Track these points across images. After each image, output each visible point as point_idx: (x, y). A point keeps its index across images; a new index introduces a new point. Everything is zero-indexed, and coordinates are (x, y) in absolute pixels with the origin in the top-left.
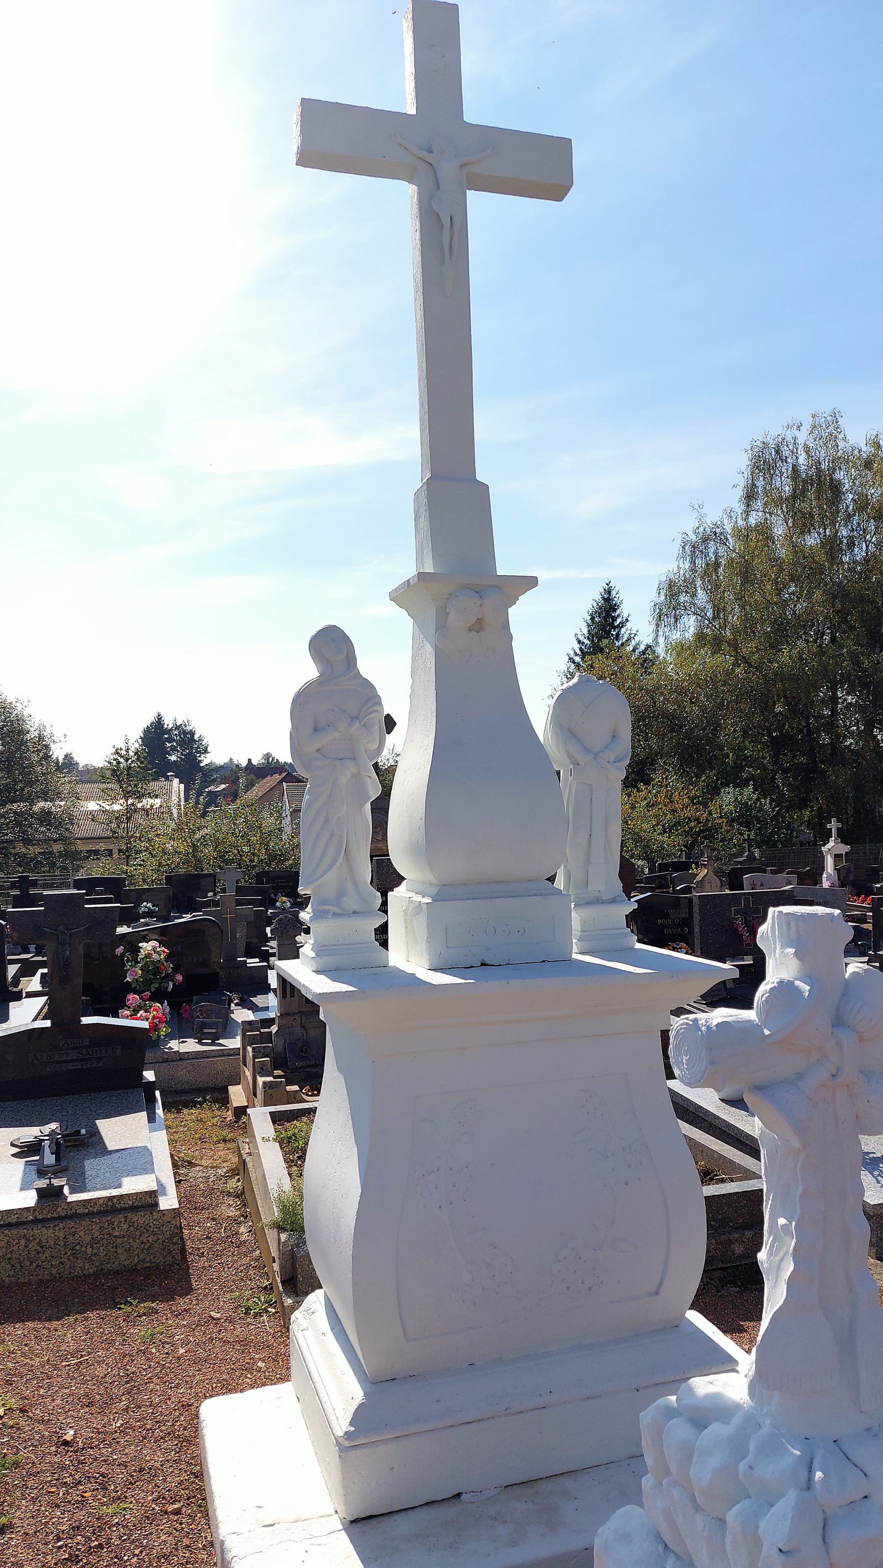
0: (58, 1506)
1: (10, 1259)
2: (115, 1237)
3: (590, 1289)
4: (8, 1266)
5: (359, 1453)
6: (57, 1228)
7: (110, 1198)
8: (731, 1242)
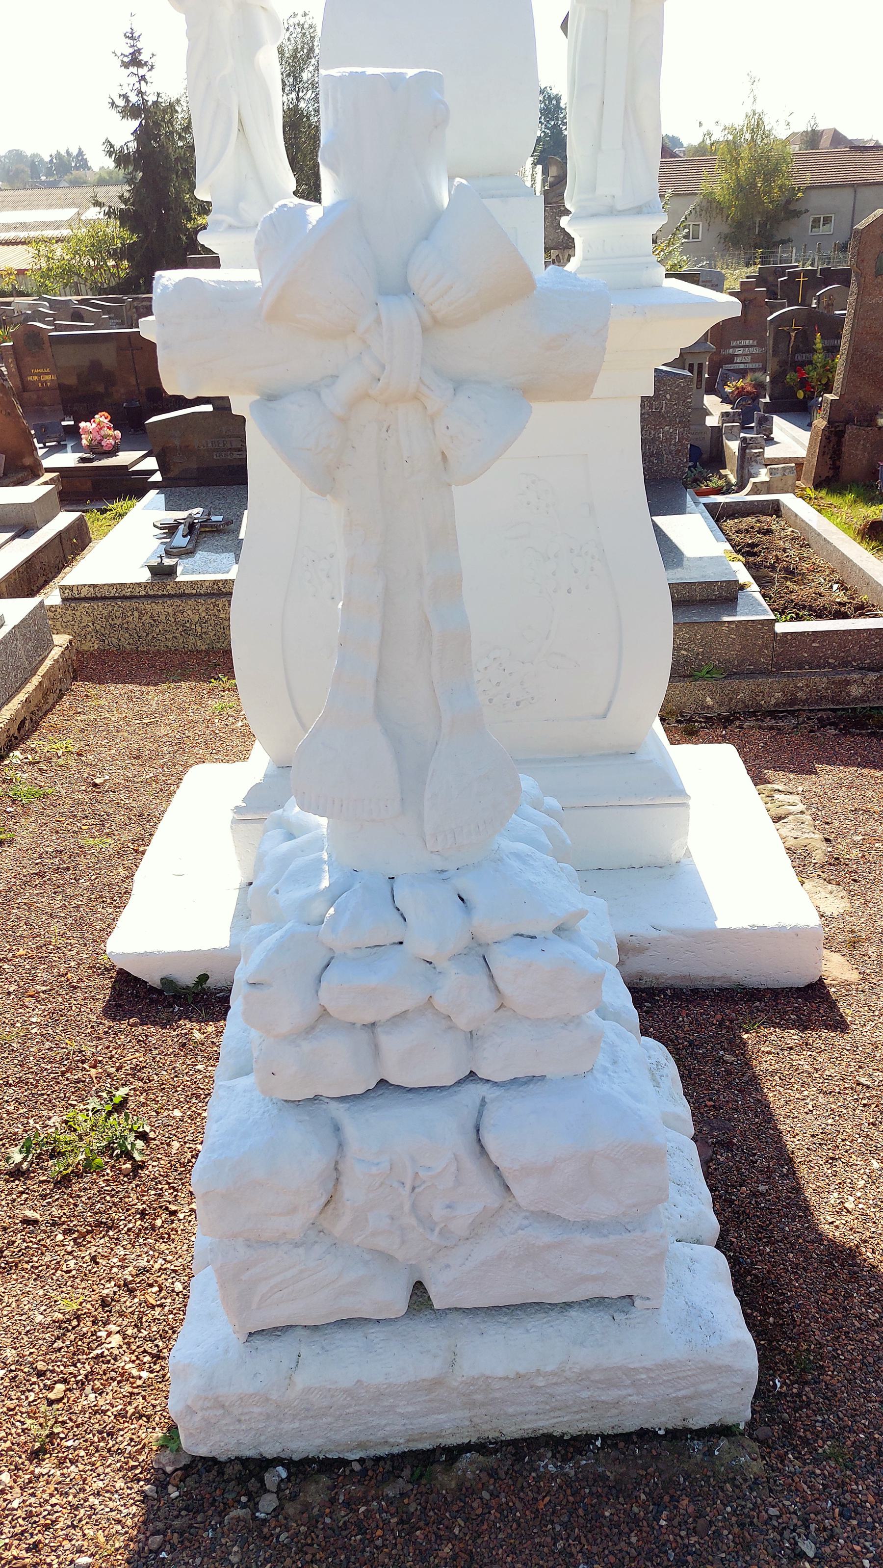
0: (57, 832)
1: (127, 628)
2: (222, 619)
3: (518, 704)
4: (127, 635)
5: (250, 826)
6: (166, 605)
7: (215, 582)
8: (848, 683)
